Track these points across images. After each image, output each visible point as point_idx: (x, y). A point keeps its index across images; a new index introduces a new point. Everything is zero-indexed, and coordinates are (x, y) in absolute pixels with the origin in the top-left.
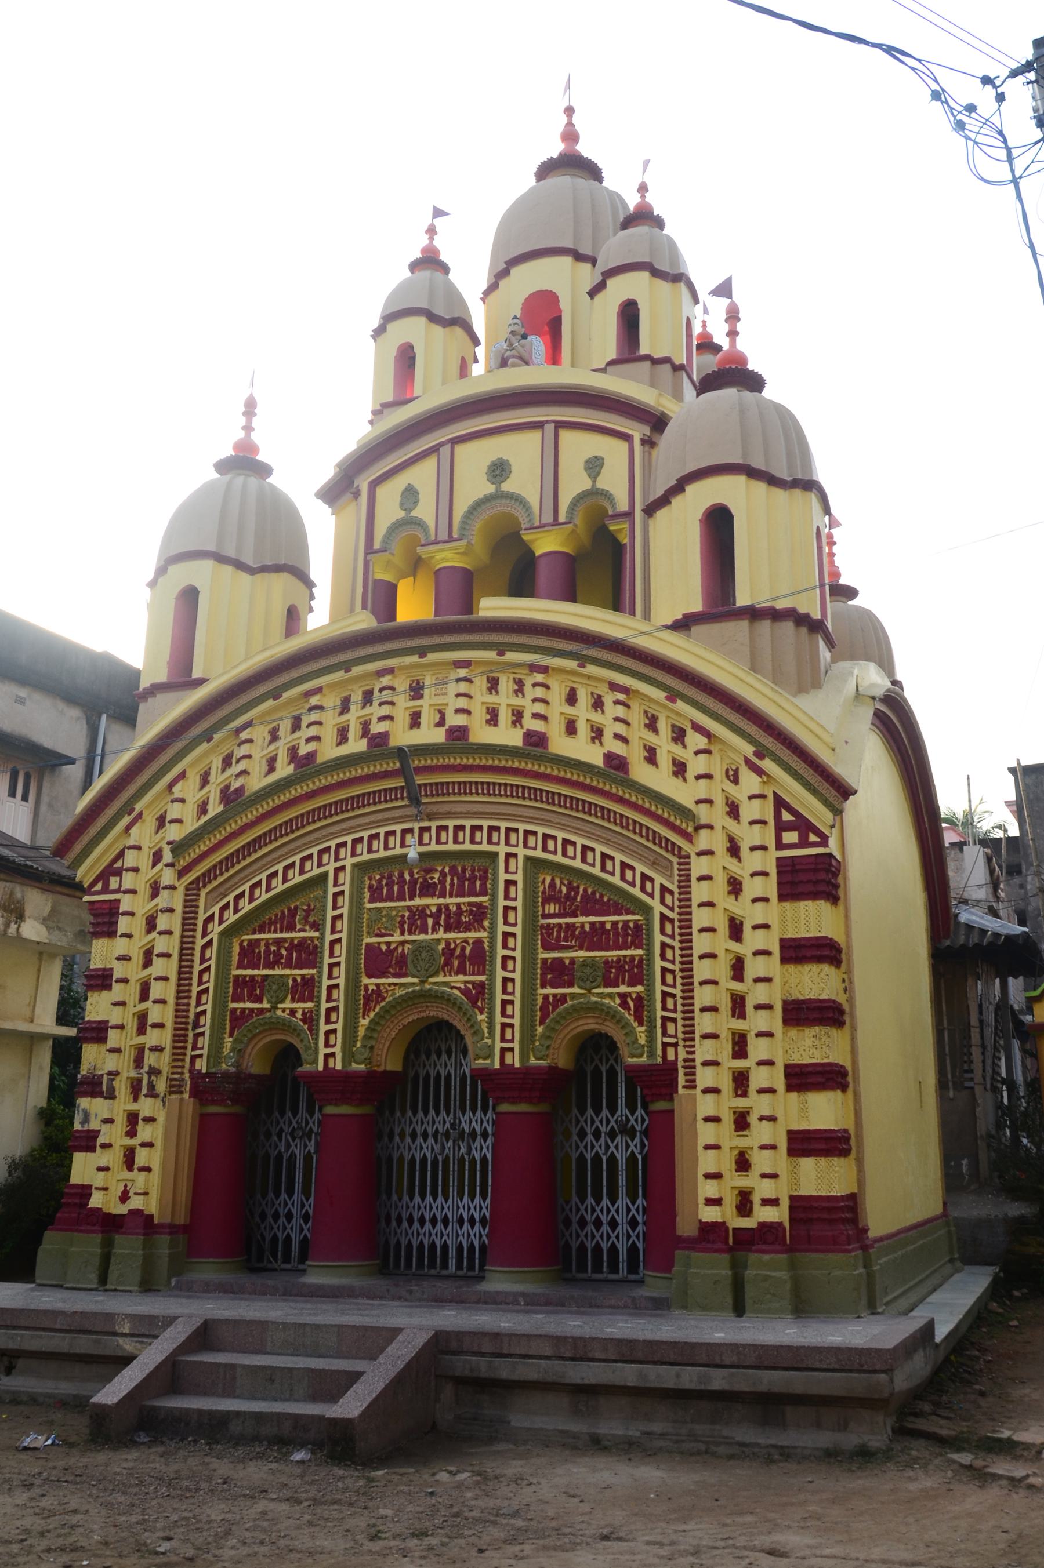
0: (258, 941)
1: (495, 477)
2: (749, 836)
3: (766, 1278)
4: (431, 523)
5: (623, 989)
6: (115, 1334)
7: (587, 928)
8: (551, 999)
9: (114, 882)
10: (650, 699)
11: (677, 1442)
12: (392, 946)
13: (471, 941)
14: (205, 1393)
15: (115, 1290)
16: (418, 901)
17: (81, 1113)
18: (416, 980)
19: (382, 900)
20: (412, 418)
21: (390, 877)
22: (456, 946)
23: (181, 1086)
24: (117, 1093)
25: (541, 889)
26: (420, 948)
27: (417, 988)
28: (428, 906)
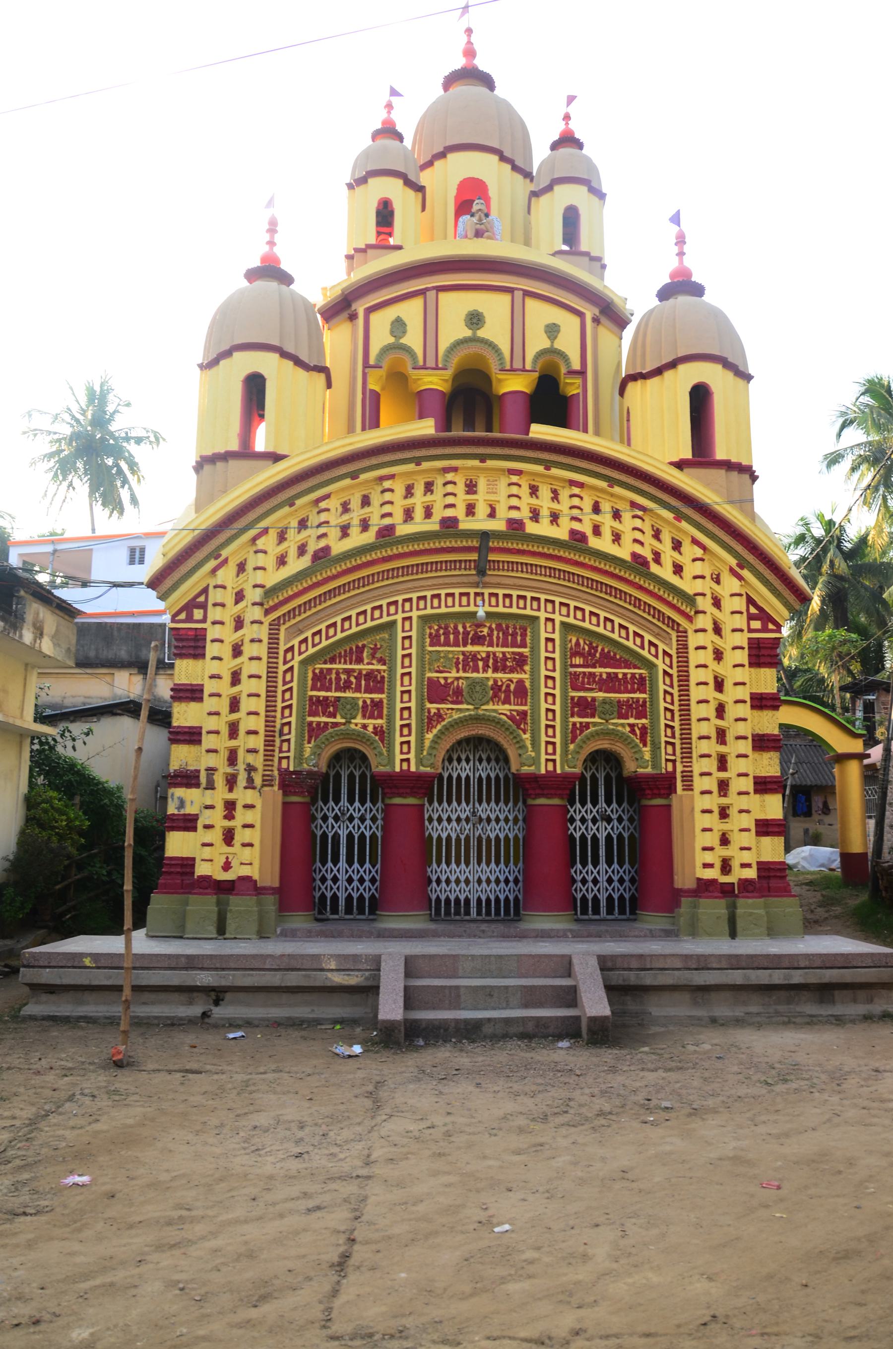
0: (330, 671)
1: (472, 324)
2: (729, 622)
3: (751, 914)
4: (419, 351)
5: (632, 721)
6: (322, 970)
7: (604, 676)
8: (578, 725)
9: (198, 614)
10: (659, 517)
11: (769, 1017)
12: (449, 681)
13: (515, 681)
14: (434, 1008)
15: (235, 938)
16: (470, 648)
17: (176, 800)
18: (471, 707)
19: (440, 645)
20: (402, 265)
21: (446, 628)
22: (503, 683)
23: (272, 780)
24: (216, 785)
25: (569, 646)
26: (473, 683)
27: (472, 713)
28: (479, 652)
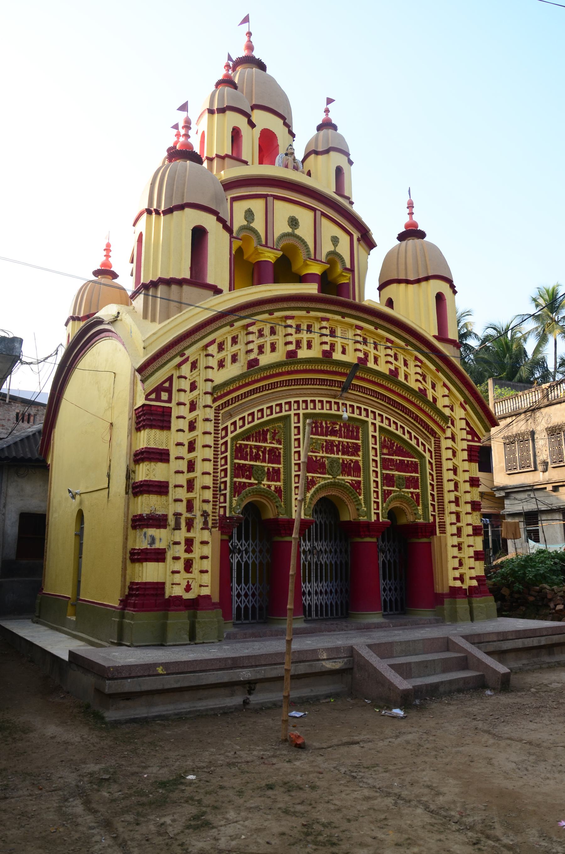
0: (246, 446)
5: (412, 490)
6: (319, 660)
10: (427, 367)
12: (318, 458)
15: (203, 643)
16: (329, 438)
26: (333, 461)
27: (332, 481)
28: (334, 441)
